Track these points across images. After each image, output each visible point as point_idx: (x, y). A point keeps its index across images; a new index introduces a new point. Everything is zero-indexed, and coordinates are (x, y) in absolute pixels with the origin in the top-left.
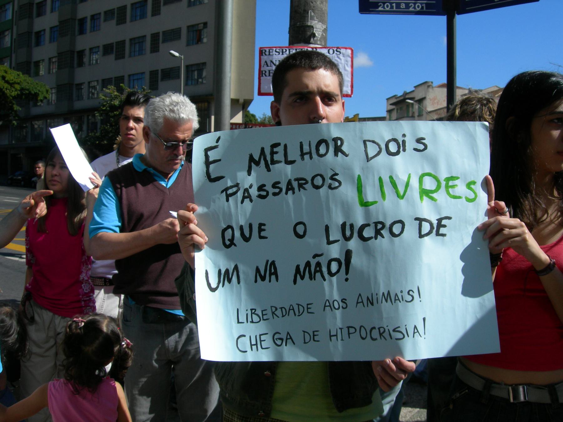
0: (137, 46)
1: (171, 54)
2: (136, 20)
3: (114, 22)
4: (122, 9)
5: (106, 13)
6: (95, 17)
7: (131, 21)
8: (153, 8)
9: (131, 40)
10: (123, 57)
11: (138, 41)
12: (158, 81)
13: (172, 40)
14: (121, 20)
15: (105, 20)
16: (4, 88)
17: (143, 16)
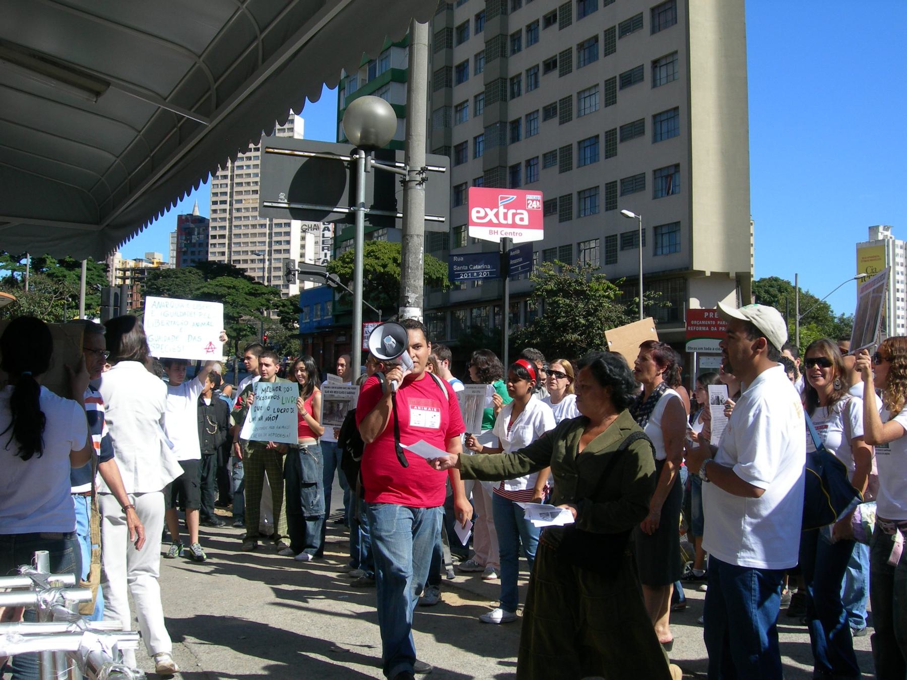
0: (588, 201)
1: (623, 214)
2: (585, 165)
3: (556, 168)
4: (566, 151)
5: (545, 155)
6: (532, 163)
7: (579, 167)
8: (606, 146)
9: (579, 193)
10: (570, 218)
11: (587, 195)
12: (616, 251)
13: (633, 191)
14: (566, 167)
15: (545, 167)
16: (395, 272)
17: (594, 159)
